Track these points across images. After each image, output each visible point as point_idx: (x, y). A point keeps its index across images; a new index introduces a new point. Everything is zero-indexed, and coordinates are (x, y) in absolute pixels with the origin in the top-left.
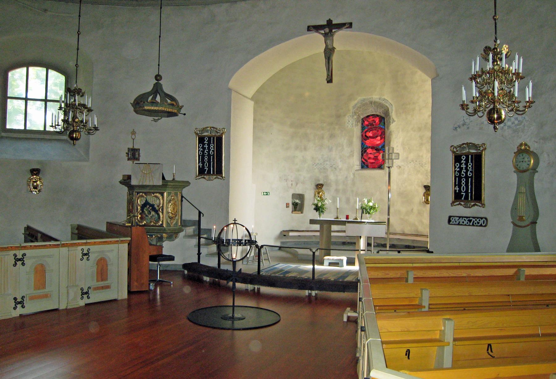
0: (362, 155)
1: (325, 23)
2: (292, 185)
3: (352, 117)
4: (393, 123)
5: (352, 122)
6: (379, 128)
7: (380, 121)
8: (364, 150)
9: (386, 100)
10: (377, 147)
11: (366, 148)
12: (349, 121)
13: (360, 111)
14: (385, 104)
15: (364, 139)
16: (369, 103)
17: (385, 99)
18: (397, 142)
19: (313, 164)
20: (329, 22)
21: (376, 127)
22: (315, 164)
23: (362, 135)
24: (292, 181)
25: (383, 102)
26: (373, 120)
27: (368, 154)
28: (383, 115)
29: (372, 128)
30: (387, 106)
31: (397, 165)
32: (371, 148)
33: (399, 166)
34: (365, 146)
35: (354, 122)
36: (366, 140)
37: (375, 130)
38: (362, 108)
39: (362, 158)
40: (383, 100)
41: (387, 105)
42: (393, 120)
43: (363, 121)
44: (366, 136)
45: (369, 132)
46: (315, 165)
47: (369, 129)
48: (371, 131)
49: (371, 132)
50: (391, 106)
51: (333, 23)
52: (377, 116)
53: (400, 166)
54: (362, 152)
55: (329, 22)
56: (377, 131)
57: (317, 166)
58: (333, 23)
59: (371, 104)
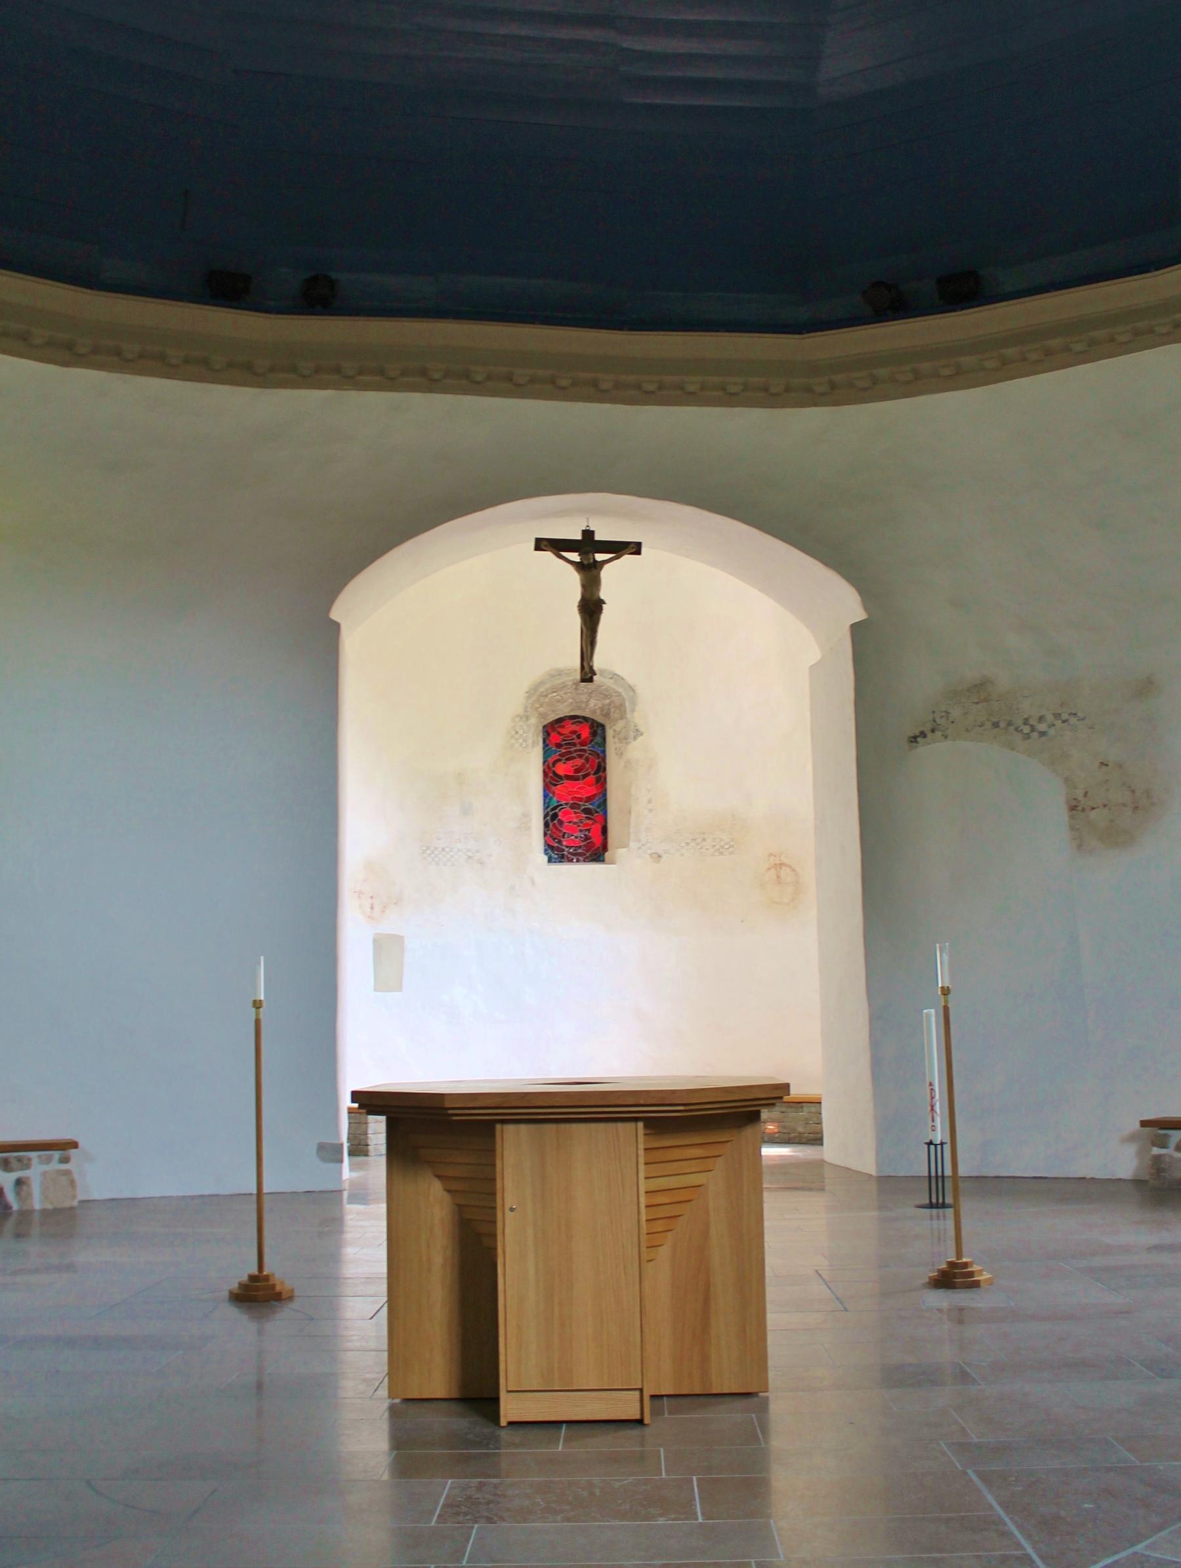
0: (546, 825)
1: (579, 537)
2: (372, 908)
3: (524, 719)
4: (635, 738)
6: (590, 754)
7: (594, 734)
8: (551, 813)
10: (588, 806)
12: (517, 733)
13: (541, 706)
14: (614, 687)
17: (615, 674)
18: (649, 791)
19: (424, 848)
20: (588, 534)
21: (580, 750)
22: (428, 848)
24: (372, 897)
25: (612, 681)
26: (574, 732)
27: (561, 822)
28: (600, 719)
29: (570, 752)
30: (619, 695)
31: (650, 852)
33: (656, 853)
34: (554, 803)
35: (530, 735)
37: (581, 756)
39: (545, 834)
40: (611, 676)
41: (620, 690)
42: (637, 730)
44: (554, 773)
46: (429, 852)
47: (562, 755)
48: (568, 759)
50: (631, 694)
51: (597, 537)
52: (585, 719)
55: (588, 534)
56: (585, 760)
57: (433, 856)
58: (597, 537)
59: (574, 687)
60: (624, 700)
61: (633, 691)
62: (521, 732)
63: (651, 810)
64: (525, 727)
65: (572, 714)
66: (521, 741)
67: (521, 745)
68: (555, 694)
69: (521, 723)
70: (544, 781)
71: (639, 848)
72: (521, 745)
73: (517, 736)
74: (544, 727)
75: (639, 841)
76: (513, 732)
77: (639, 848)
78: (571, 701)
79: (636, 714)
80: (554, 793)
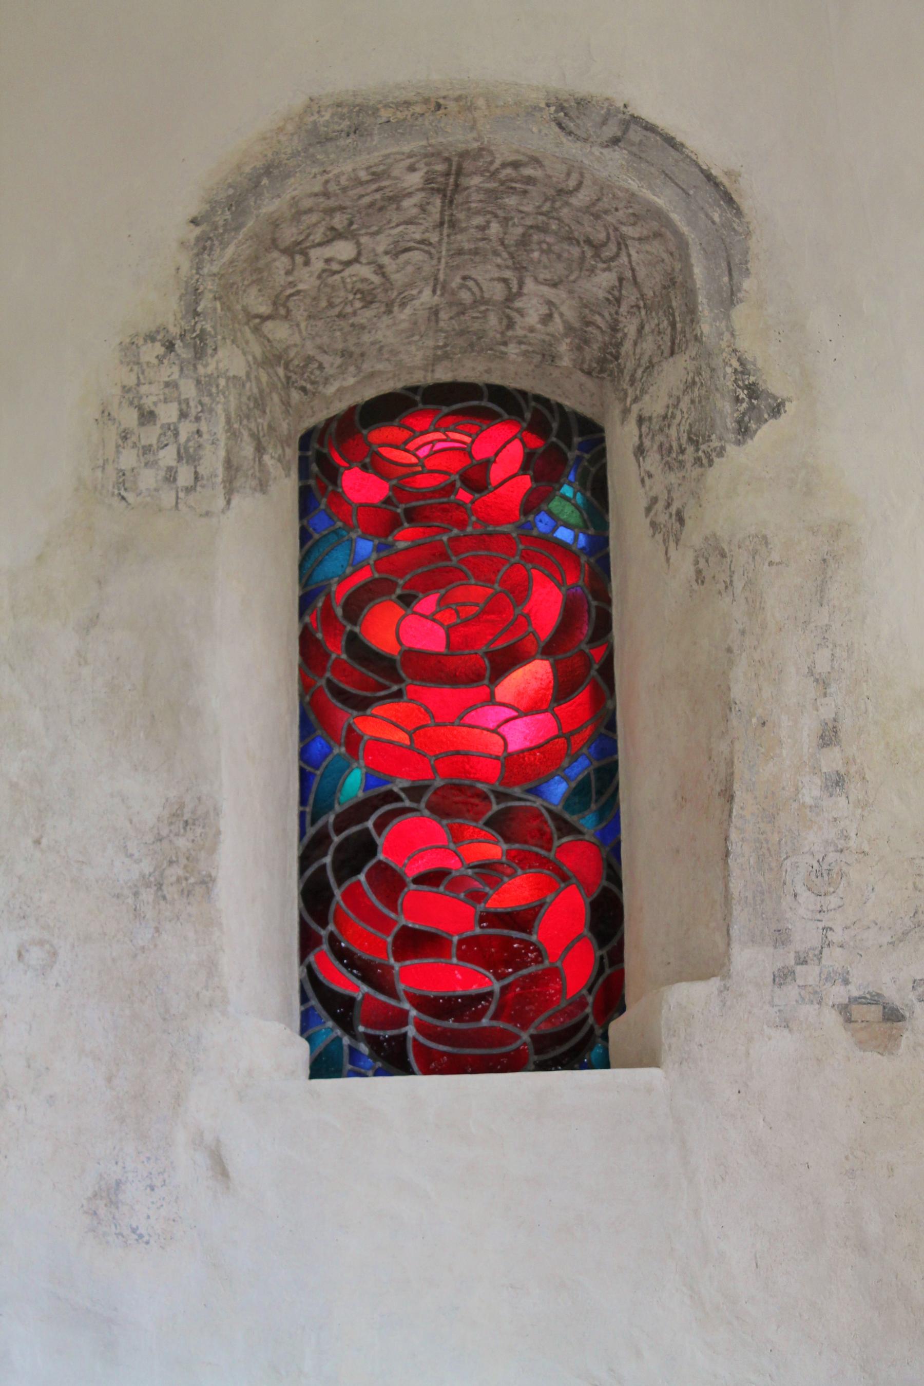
4: (744, 431)
5: (186, 429)
6: (526, 556)
8: (336, 839)
9: (650, 128)
11: (360, 810)
12: (147, 417)
15: (339, 693)
16: (415, 179)
17: (635, 119)
18: (823, 684)
21: (482, 541)
23: (307, 641)
25: (617, 156)
31: (838, 993)
32: (439, 809)
33: (874, 999)
36: (362, 704)
38: (317, 256)
39: (307, 941)
40: (612, 130)
42: (753, 391)
43: (322, 459)
44: (354, 643)
45: (406, 600)
48: (428, 583)
49: (428, 602)
53: (892, 995)
54: (305, 860)
60: (683, 244)
61: (729, 200)
62: (168, 413)
63: (837, 782)
64: (188, 389)
65: (443, 375)
66: (168, 457)
67: (171, 476)
68: (344, 250)
69: (169, 372)
70: (305, 684)
71: (783, 977)
72: (171, 476)
73: (150, 435)
74: (305, 441)
75: (781, 938)
76: (130, 418)
77: (783, 977)
78: (426, 297)
79: (739, 314)
80: (352, 741)
